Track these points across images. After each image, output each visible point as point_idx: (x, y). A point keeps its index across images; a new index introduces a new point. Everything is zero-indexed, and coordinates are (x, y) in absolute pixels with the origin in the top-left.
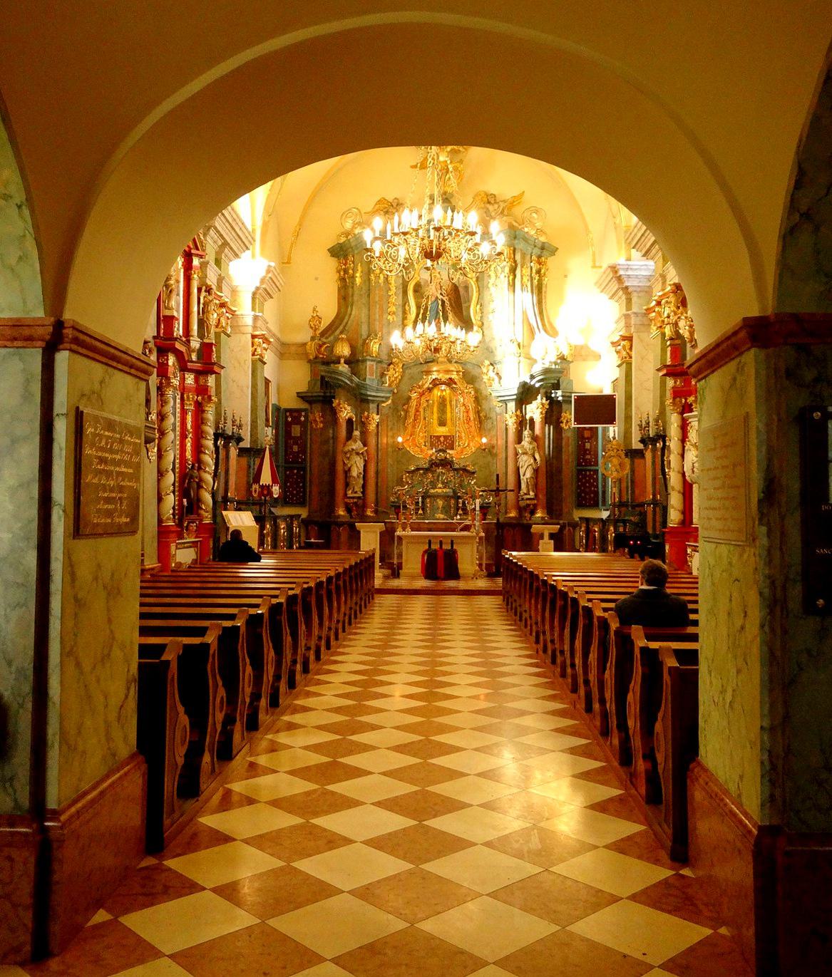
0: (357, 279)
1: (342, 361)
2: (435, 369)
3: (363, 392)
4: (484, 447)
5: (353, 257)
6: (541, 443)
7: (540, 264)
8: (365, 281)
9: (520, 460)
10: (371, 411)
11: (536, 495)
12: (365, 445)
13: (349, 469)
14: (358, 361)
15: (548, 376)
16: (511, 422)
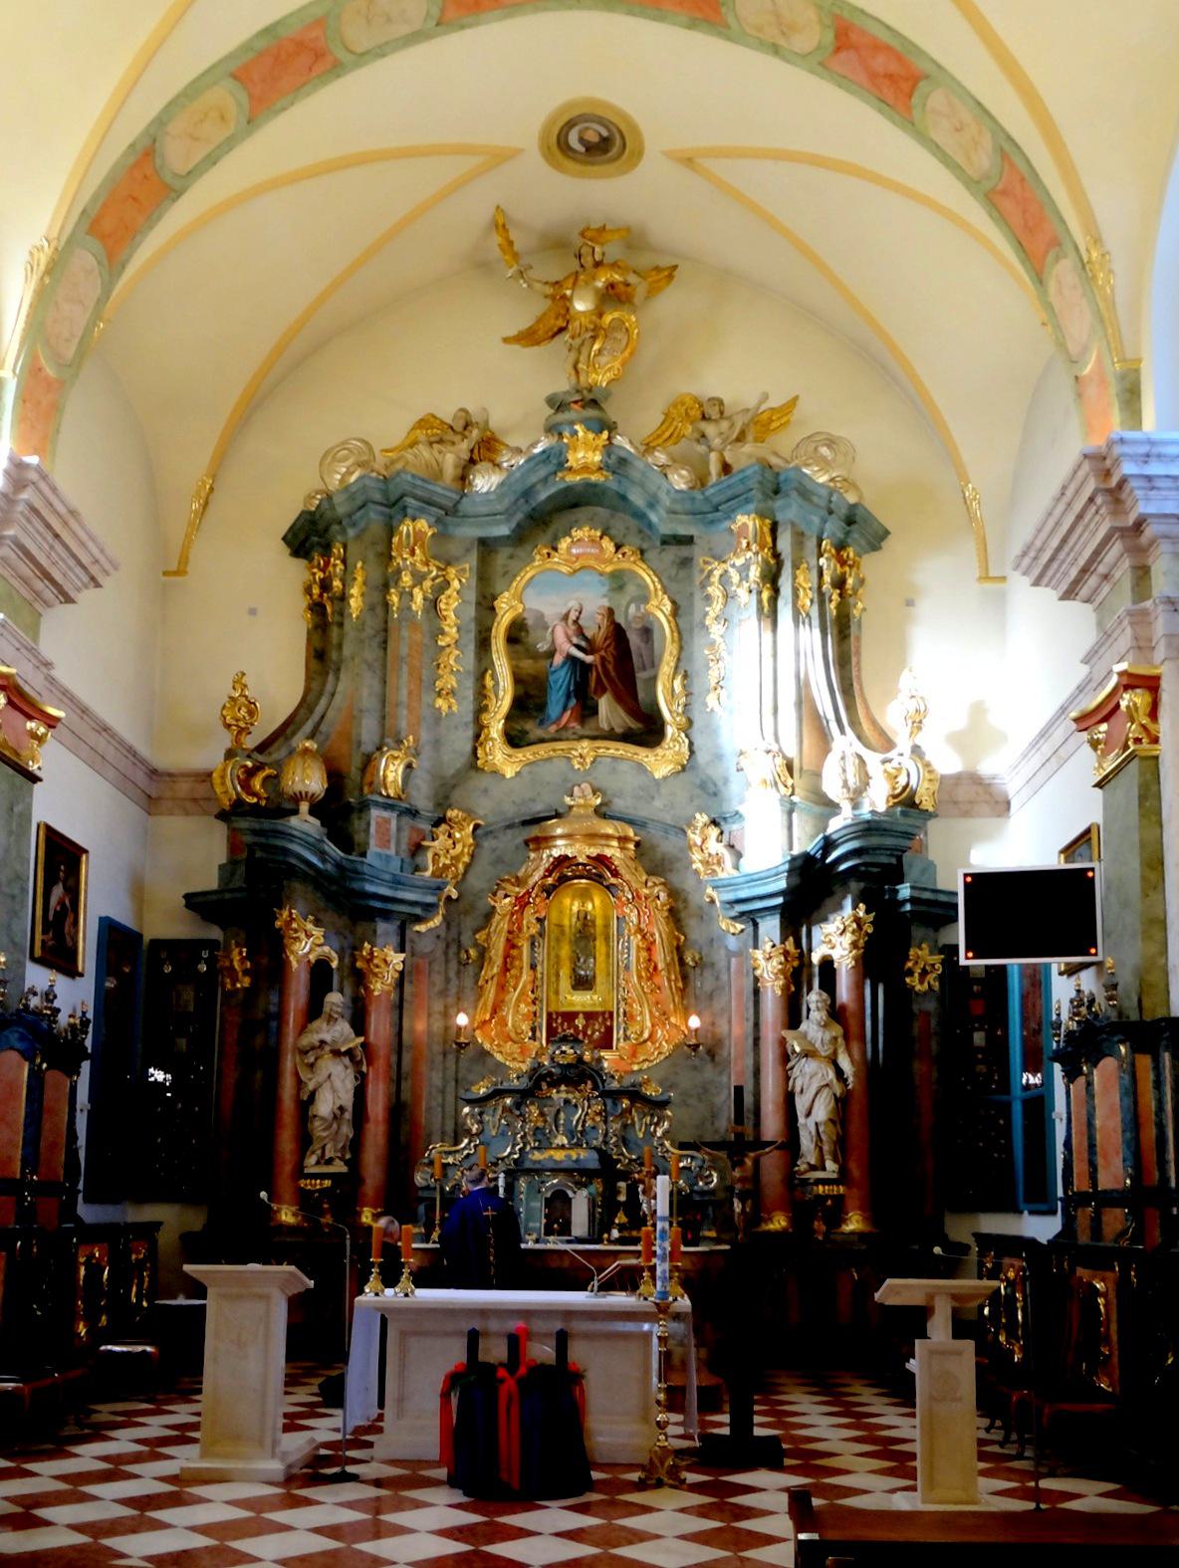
0: (352, 602)
1: (304, 807)
2: (559, 831)
3: (356, 885)
4: (693, 1041)
5: (345, 547)
6: (853, 1023)
7: (843, 563)
8: (372, 608)
9: (796, 1072)
10: (380, 941)
13: (313, 1095)
14: (349, 809)
15: (875, 841)
16: (768, 966)
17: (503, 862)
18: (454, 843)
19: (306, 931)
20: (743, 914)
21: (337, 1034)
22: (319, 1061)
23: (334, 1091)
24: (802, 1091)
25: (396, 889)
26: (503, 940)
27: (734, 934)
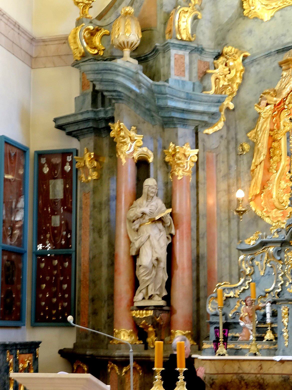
3: (161, 103)
10: (180, 141)
12: (169, 204)
14: (155, 50)
17: (264, 81)
18: (229, 70)
19: (130, 137)
21: (153, 208)
22: (142, 227)
23: (152, 247)
25: (190, 103)
26: (266, 136)
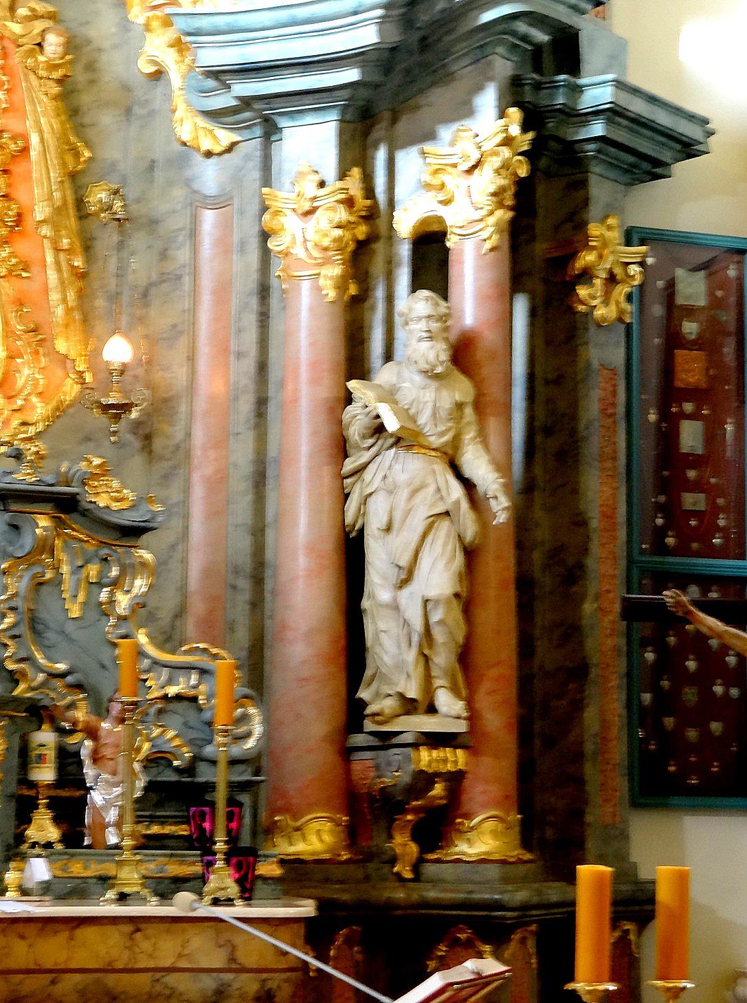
11: (473, 717)
20: (246, 102)
24: (388, 529)
27: (209, 154)
